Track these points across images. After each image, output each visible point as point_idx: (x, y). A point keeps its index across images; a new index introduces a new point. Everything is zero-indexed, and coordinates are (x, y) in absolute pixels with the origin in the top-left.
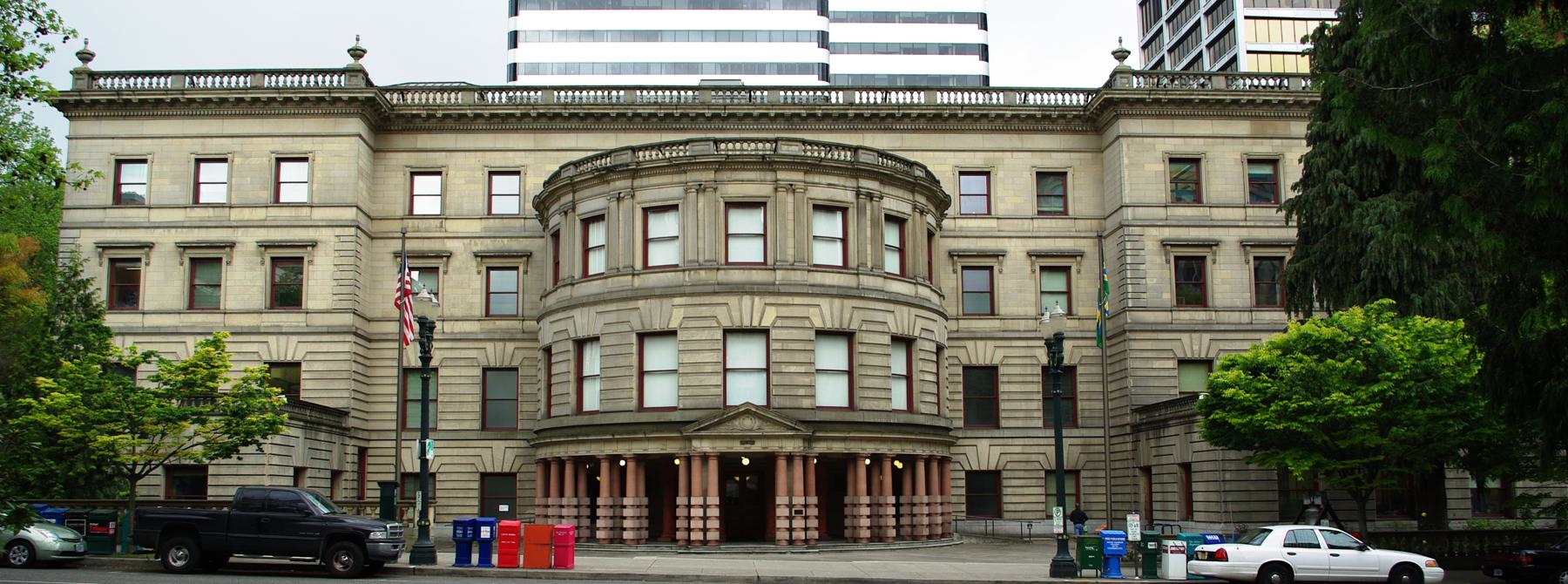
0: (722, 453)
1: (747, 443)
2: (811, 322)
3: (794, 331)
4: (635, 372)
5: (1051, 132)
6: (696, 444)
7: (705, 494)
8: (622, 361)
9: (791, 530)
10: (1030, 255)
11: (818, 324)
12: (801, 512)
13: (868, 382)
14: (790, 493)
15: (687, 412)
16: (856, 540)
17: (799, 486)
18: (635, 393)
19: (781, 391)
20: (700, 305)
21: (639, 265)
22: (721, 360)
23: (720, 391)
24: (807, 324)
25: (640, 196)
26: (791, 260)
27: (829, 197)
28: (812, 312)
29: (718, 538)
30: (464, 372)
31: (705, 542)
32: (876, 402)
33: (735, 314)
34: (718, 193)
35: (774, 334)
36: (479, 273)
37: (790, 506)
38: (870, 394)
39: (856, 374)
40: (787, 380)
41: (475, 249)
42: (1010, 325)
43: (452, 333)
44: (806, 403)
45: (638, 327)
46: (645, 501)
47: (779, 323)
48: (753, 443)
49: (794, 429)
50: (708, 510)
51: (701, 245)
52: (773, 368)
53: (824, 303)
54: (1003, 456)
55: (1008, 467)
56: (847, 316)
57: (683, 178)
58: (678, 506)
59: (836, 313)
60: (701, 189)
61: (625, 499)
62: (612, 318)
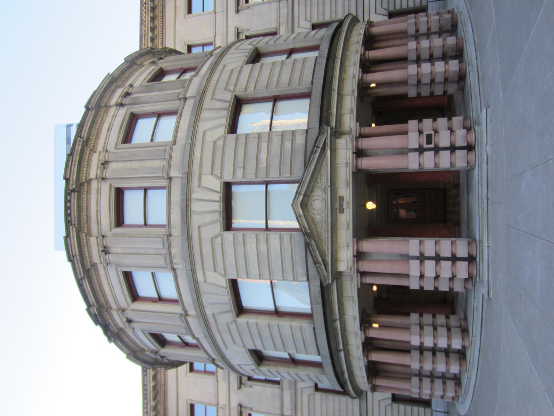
0: (354, 236)
1: (341, 205)
2: (219, 138)
3: (227, 156)
4: (275, 321)
5: (163, 8)
6: (342, 267)
7: (407, 258)
9: (453, 148)
10: (238, 11)
11: (222, 131)
12: (429, 137)
13: (285, 79)
14: (404, 151)
15: (310, 273)
16: (462, 77)
17: (395, 142)
18: (296, 323)
19: (286, 167)
20: (201, 255)
21: (177, 309)
22: (253, 235)
23: (286, 235)
24: (220, 143)
25: (123, 304)
26: (164, 163)
27: (118, 129)
28: (211, 137)
30: (318, 406)
31: (471, 259)
32: (306, 70)
33: (209, 218)
34: (109, 234)
35: (228, 178)
36: (251, 386)
37: (421, 150)
38: (297, 76)
39: (277, 94)
40: (275, 163)
41: (236, 388)
42: (283, 19)
43: (291, 410)
44: (300, 140)
45: (230, 316)
46: (414, 317)
47: (217, 172)
48: (341, 199)
49: (323, 149)
50: (426, 255)
51: (152, 251)
52: (263, 178)
53: (202, 126)
54: (378, 12)
55: (385, 6)
56: (218, 104)
57: (100, 267)
58: (422, 288)
59: (214, 114)
60: (106, 251)
62: (227, 337)
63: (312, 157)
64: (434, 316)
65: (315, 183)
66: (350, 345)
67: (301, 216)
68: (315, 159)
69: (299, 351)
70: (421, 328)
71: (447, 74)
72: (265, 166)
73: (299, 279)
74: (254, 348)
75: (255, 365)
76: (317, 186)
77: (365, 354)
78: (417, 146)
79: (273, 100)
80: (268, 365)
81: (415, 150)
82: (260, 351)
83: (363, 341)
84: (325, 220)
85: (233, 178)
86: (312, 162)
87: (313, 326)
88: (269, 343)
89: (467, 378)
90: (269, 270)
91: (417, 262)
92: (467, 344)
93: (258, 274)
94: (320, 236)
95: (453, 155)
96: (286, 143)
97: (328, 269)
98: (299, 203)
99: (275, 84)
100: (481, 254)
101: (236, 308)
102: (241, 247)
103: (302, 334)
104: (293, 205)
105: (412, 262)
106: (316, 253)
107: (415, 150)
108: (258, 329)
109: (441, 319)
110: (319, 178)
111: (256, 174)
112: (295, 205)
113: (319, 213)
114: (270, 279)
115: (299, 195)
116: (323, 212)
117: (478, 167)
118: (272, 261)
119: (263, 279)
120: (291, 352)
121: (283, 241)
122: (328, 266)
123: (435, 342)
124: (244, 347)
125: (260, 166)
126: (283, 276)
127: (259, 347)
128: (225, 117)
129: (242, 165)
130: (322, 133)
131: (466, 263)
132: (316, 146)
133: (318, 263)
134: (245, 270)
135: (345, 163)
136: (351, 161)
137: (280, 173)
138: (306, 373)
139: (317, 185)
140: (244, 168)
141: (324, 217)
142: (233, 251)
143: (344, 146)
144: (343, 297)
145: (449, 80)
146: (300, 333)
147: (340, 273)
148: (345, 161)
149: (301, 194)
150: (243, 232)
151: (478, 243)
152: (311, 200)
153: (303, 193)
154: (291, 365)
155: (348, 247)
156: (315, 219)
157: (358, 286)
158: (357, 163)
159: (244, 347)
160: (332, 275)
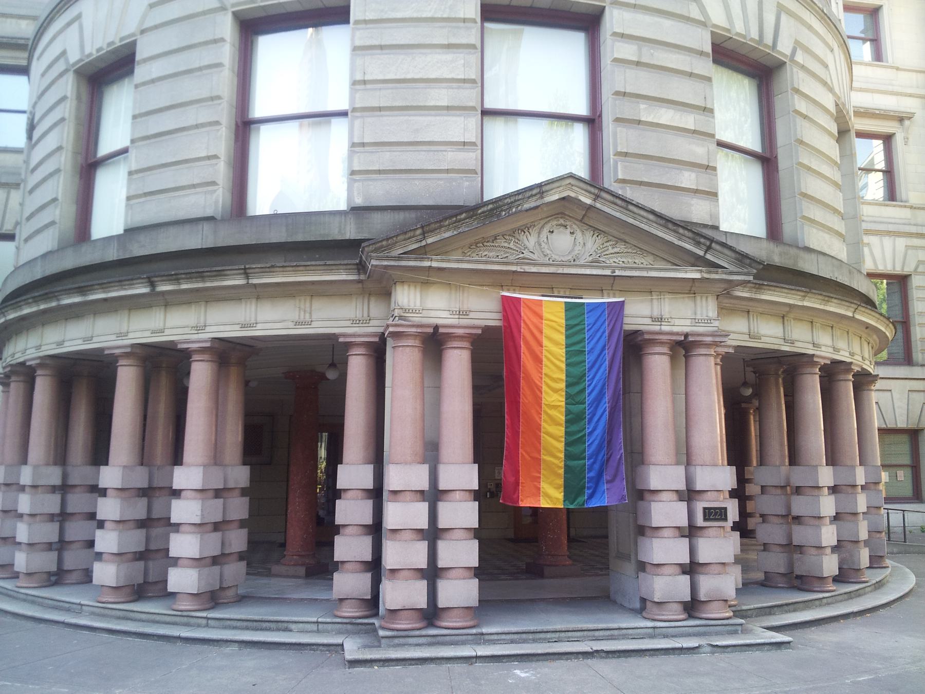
3: (667, 23)
8: (191, 89)
9: (692, 568)
15: (377, 217)
18: (221, 171)
29: (474, 602)
37: (689, 495)
40: (650, 144)
61: (178, 472)
63: (686, 232)
64: (242, 524)
65: (614, 239)
66: (206, 307)
67: (542, 198)
68: (680, 239)
69: (135, 176)
70: (218, 493)
71: (813, 551)
72: (643, 119)
73: (356, 185)
74: (138, 57)
75: (81, 60)
76: (608, 244)
77: (138, 351)
78: (699, 486)
79: (768, 155)
80: (79, 98)
81: (689, 480)
82: (131, 72)
83: (180, 346)
84: (524, 258)
85: (615, 34)
86: (675, 231)
87: (219, 217)
88: (158, 97)
89: (80, 604)
90: (380, 109)
91: (424, 485)
92: (184, 605)
93: (367, 77)
94: (485, 244)
95: (678, 570)
96: (693, 175)
97: (409, 259)
98: (573, 195)
99: (806, 162)
100: (448, 638)
101: (262, 14)
102: (440, 36)
103: (194, 186)
104: (571, 176)
105: (424, 470)
106: (448, 230)
107: (689, 480)
108: (200, 69)
109: (238, 540)
110: (626, 250)
111: (624, 94)
112: (570, 184)
113: (543, 245)
114: (354, 110)
115: (594, 194)
116: (545, 256)
117: (654, 628)
118: (406, 118)
119: (353, 92)
120: (132, 154)
121: (460, 150)
122: (416, 259)
123: (182, 528)
124: (143, 32)
125: (642, 106)
126: (363, 145)
127: (141, 73)
128: (746, 32)
129: (644, 60)
130: (740, 261)
131: (422, 602)
132: (711, 244)
133: (424, 235)
134: (376, 43)
135: (661, 315)
136: (665, 328)
137: (626, 154)
138: (60, 197)
139: (611, 243)
140: (638, 64)
141: (531, 256)
142: (429, 15)
143: (702, 315)
144: (308, 298)
145: (796, 556)
146: (196, 181)
147: (386, 294)
148: (666, 315)
149: (595, 200)
150: (479, 45)
151: (474, 631)
152: (574, 226)
153: (598, 205)
154: (80, 159)
155: (459, 314)
156: (527, 233)
157: (344, 335)
158: (662, 343)
159: (143, 32)
160: (386, 267)
